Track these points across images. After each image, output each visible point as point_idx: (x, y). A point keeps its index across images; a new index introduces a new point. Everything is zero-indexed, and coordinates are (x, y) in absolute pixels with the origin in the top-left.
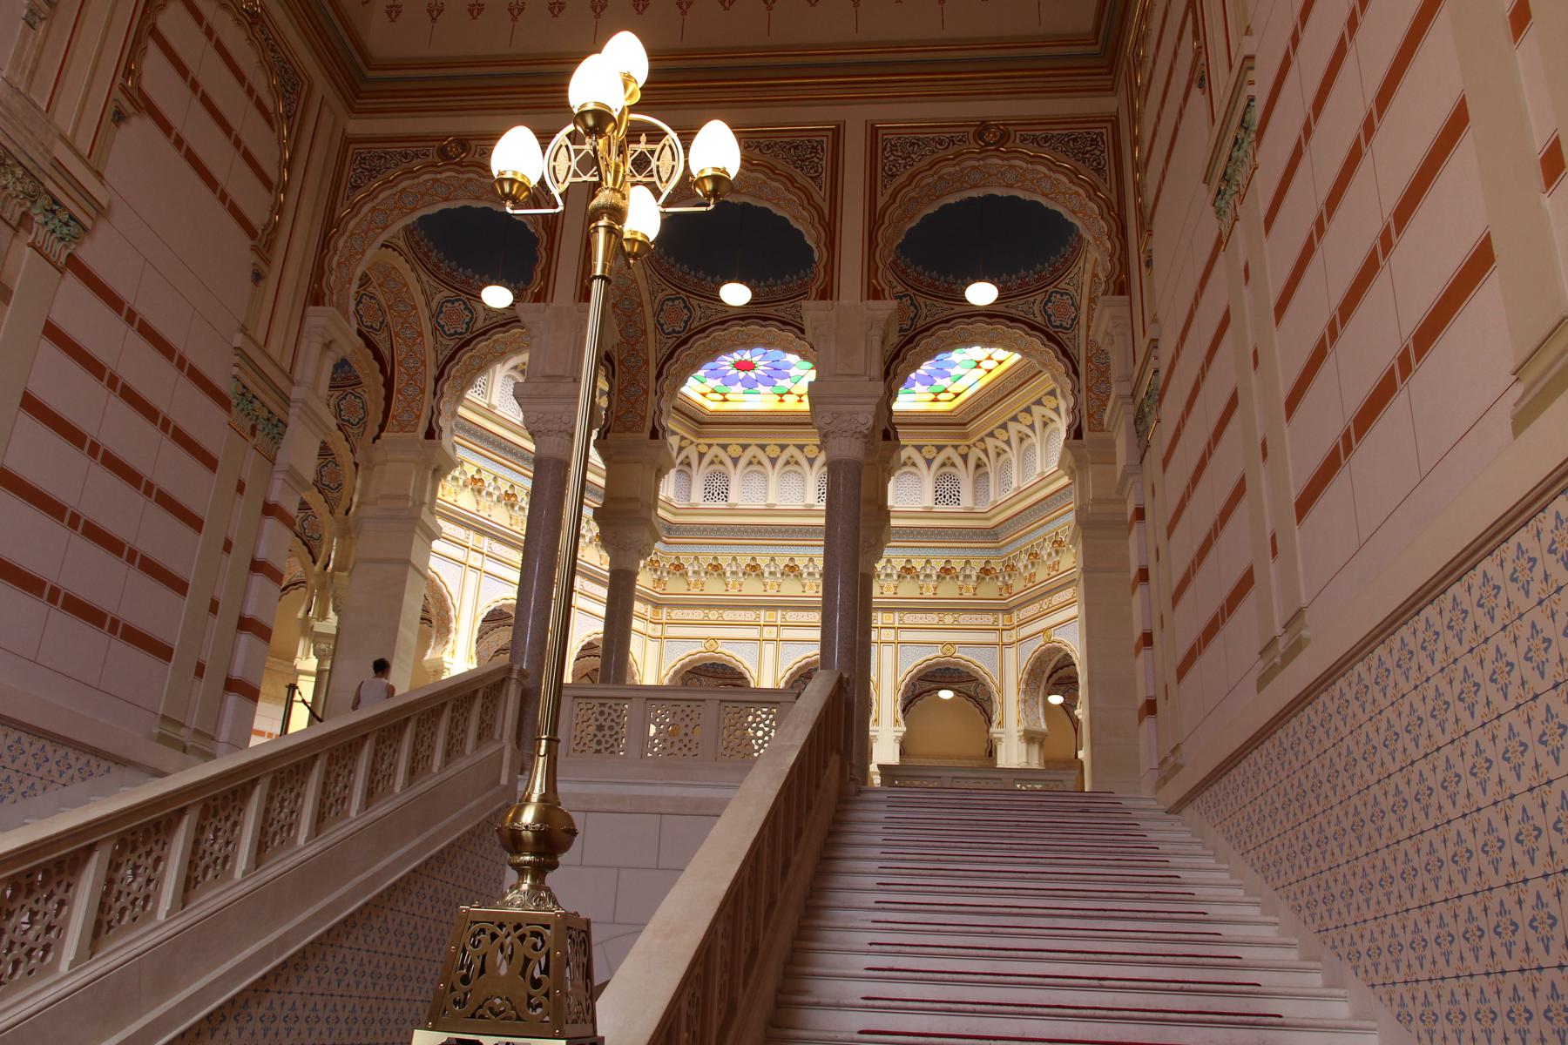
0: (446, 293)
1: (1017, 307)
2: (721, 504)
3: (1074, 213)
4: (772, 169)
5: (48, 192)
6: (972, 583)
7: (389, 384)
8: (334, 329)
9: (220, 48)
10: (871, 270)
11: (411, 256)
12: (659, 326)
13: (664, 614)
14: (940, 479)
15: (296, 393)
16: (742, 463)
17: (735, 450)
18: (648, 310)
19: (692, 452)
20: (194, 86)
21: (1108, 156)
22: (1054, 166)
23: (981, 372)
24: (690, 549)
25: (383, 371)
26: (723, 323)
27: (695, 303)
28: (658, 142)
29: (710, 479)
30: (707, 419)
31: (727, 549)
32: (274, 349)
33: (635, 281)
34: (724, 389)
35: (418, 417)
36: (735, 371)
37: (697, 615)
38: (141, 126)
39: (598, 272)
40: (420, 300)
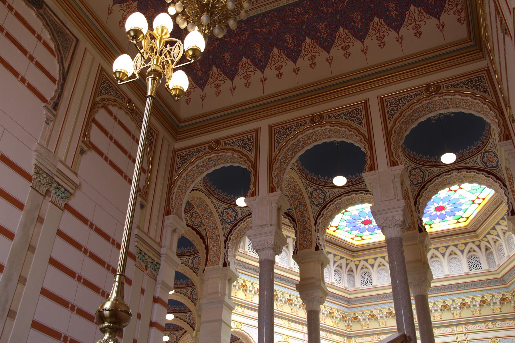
0: (224, 206)
1: (469, 163)
2: (369, 286)
3: (479, 112)
4: (341, 124)
5: (56, 181)
6: (498, 306)
7: (207, 248)
8: (178, 225)
9: (120, 123)
10: (390, 154)
11: (207, 193)
12: (312, 202)
14: (469, 259)
15: (162, 251)
16: (376, 266)
17: (371, 261)
18: (306, 196)
19: (352, 265)
20: (111, 138)
21: (488, 84)
22: (463, 94)
23: (475, 206)
24: (359, 309)
25: (204, 242)
26: (339, 196)
27: (326, 190)
28: (173, 46)
29: (363, 275)
30: (356, 249)
31: (376, 307)
32: (152, 234)
33: (297, 185)
34: (361, 235)
35: (219, 258)
36: (363, 226)
38: (91, 155)
39: (149, 94)
40: (214, 210)
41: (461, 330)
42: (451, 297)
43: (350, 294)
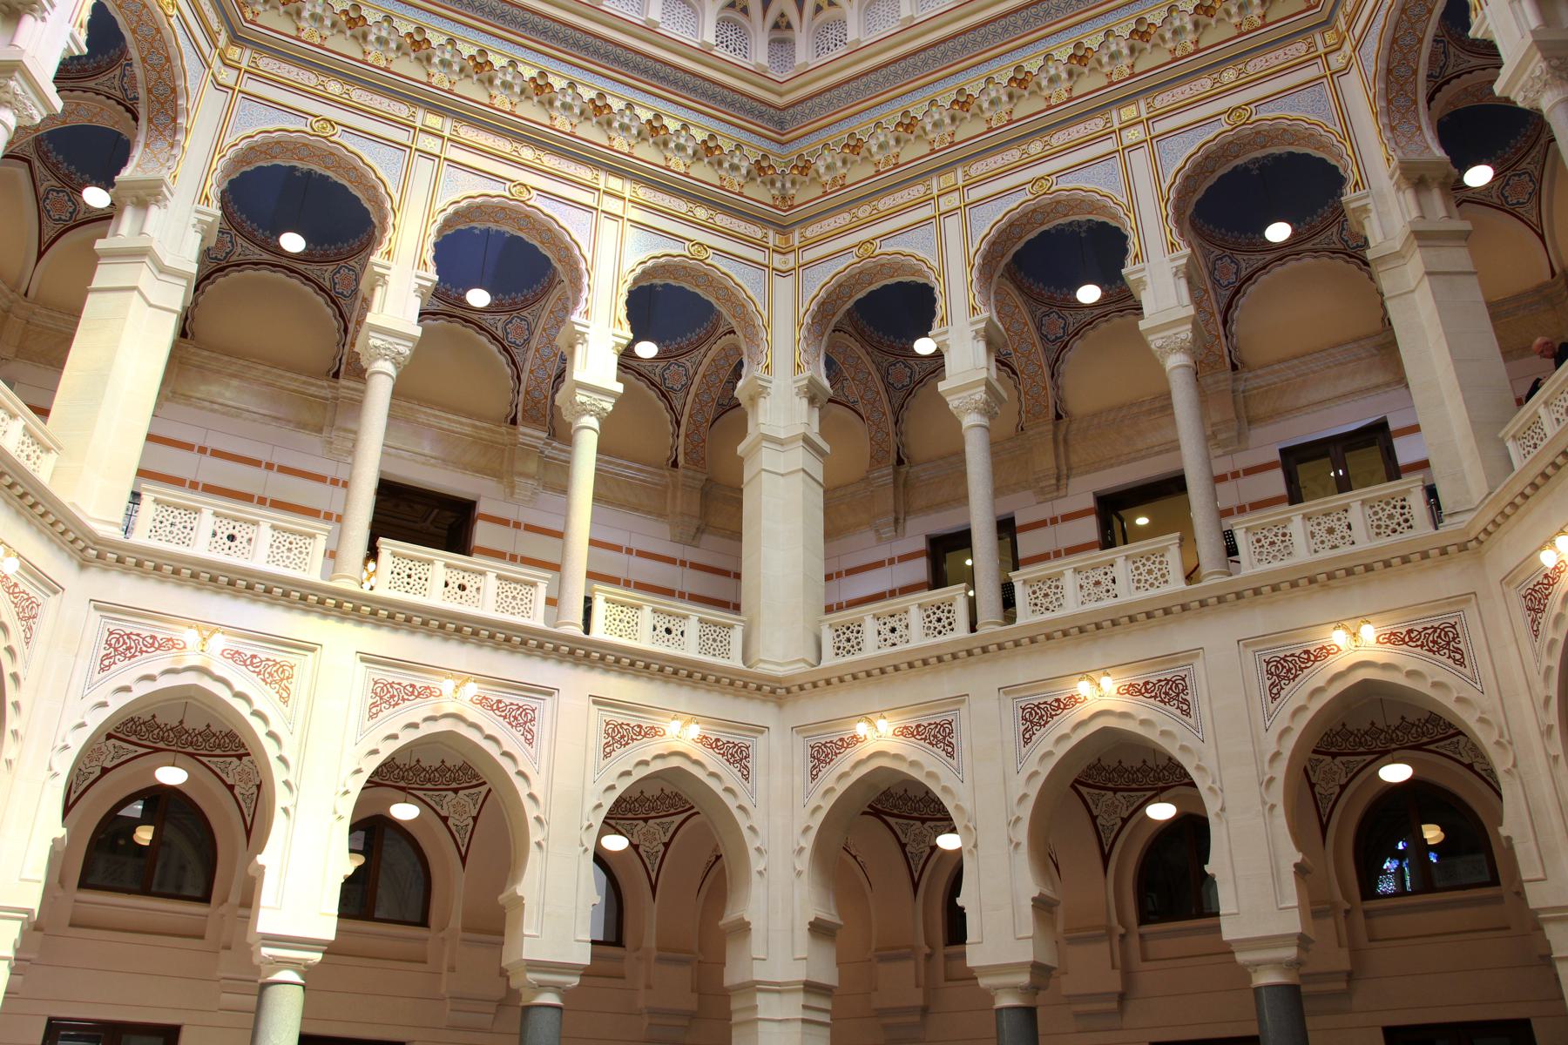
2: (842, 50)
37: (843, 219)
43: (781, 95)
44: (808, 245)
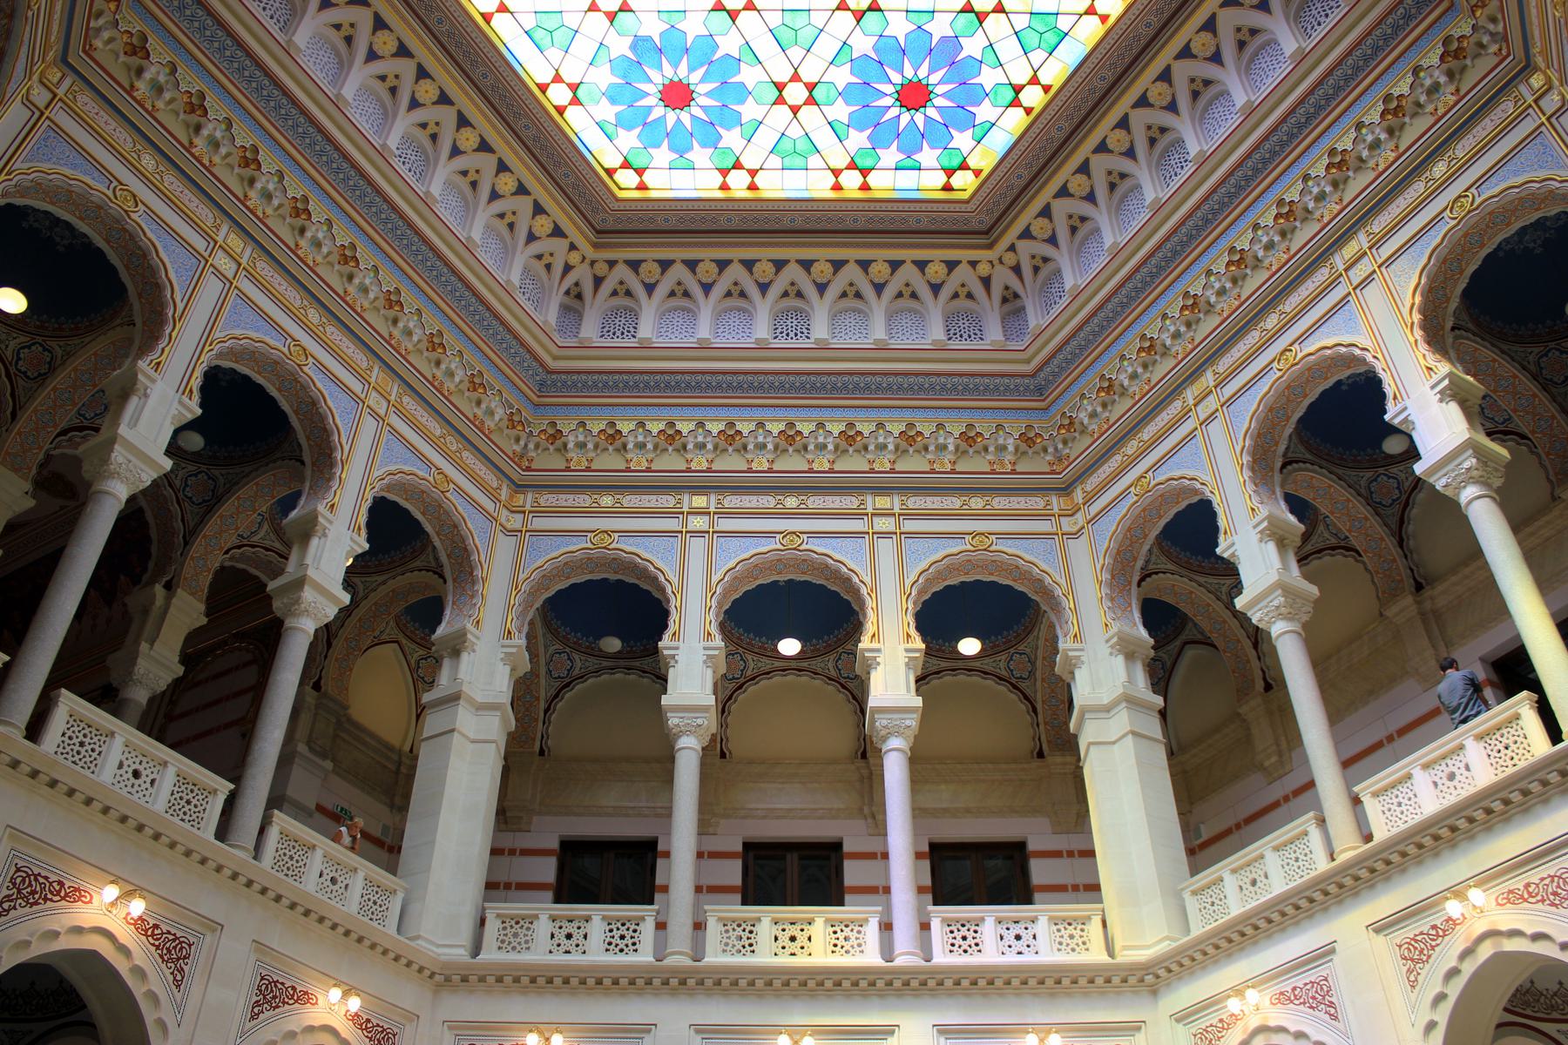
13: (527, 500)
41: (888, 506)
42: (875, 415)
44: (539, 512)
